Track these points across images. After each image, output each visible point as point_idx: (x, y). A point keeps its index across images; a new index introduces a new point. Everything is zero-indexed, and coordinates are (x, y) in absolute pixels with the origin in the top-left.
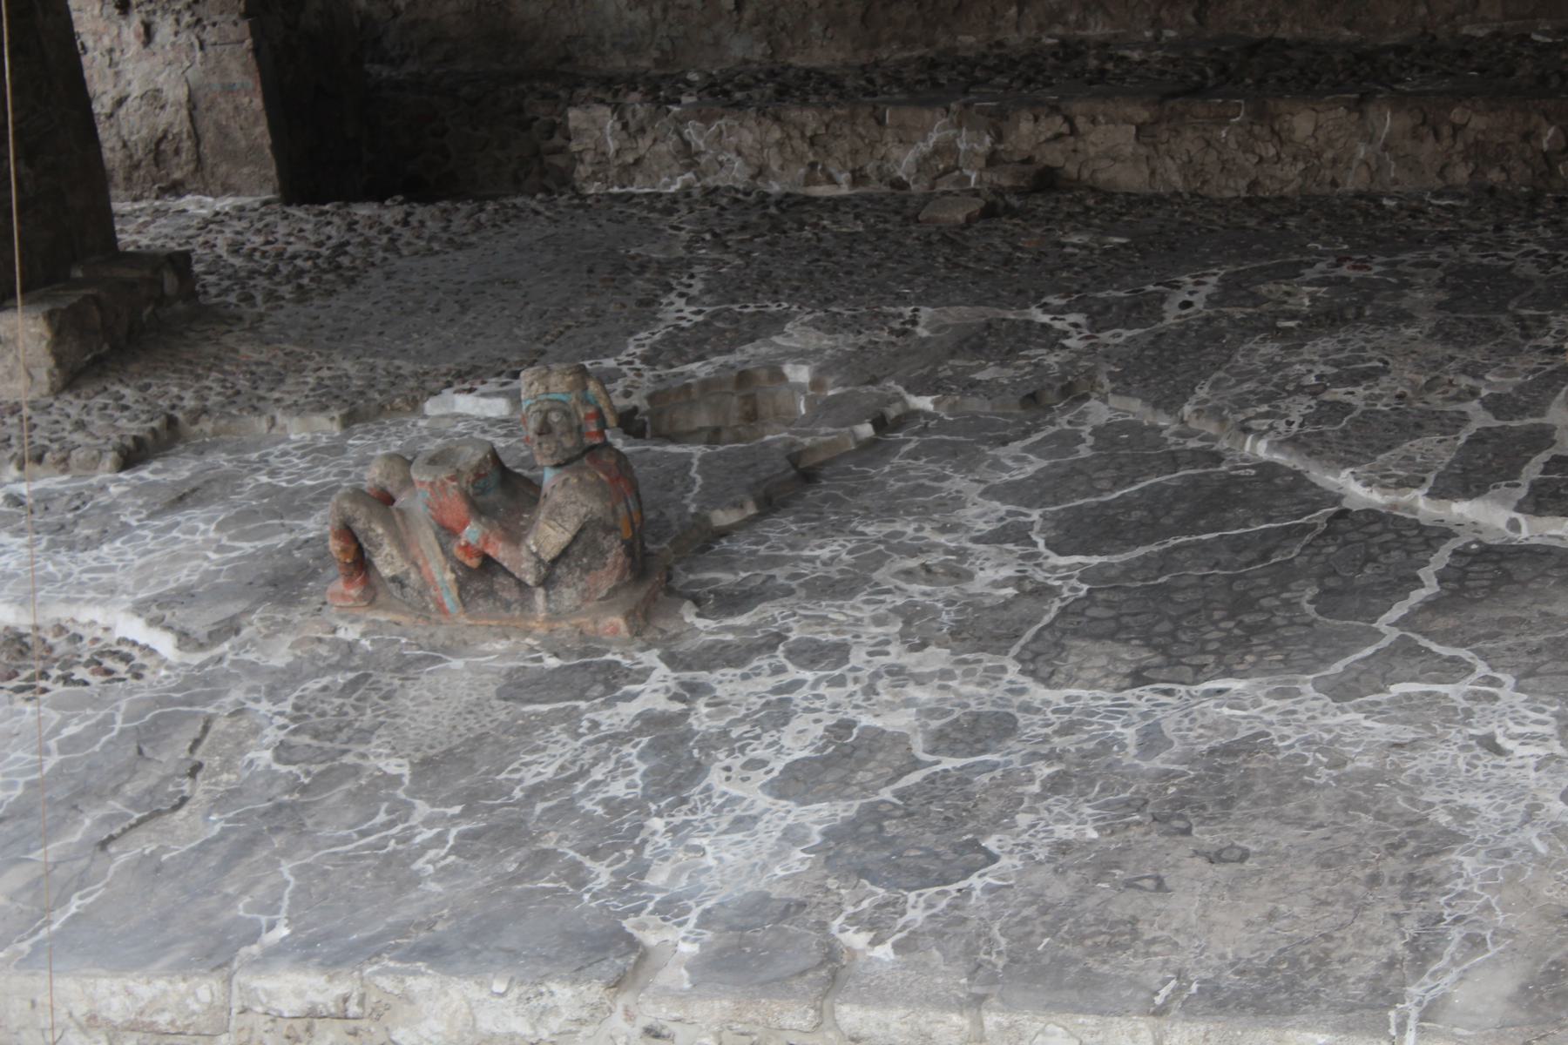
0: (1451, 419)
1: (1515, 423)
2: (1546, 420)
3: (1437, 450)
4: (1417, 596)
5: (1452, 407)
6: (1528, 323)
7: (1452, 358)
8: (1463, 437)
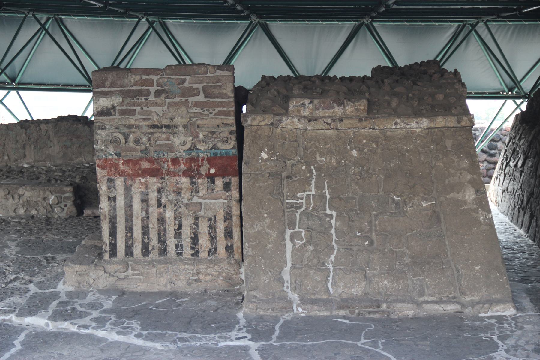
0: (24, 290)
1: (46, 291)
4: (13, 351)
6: (49, 258)
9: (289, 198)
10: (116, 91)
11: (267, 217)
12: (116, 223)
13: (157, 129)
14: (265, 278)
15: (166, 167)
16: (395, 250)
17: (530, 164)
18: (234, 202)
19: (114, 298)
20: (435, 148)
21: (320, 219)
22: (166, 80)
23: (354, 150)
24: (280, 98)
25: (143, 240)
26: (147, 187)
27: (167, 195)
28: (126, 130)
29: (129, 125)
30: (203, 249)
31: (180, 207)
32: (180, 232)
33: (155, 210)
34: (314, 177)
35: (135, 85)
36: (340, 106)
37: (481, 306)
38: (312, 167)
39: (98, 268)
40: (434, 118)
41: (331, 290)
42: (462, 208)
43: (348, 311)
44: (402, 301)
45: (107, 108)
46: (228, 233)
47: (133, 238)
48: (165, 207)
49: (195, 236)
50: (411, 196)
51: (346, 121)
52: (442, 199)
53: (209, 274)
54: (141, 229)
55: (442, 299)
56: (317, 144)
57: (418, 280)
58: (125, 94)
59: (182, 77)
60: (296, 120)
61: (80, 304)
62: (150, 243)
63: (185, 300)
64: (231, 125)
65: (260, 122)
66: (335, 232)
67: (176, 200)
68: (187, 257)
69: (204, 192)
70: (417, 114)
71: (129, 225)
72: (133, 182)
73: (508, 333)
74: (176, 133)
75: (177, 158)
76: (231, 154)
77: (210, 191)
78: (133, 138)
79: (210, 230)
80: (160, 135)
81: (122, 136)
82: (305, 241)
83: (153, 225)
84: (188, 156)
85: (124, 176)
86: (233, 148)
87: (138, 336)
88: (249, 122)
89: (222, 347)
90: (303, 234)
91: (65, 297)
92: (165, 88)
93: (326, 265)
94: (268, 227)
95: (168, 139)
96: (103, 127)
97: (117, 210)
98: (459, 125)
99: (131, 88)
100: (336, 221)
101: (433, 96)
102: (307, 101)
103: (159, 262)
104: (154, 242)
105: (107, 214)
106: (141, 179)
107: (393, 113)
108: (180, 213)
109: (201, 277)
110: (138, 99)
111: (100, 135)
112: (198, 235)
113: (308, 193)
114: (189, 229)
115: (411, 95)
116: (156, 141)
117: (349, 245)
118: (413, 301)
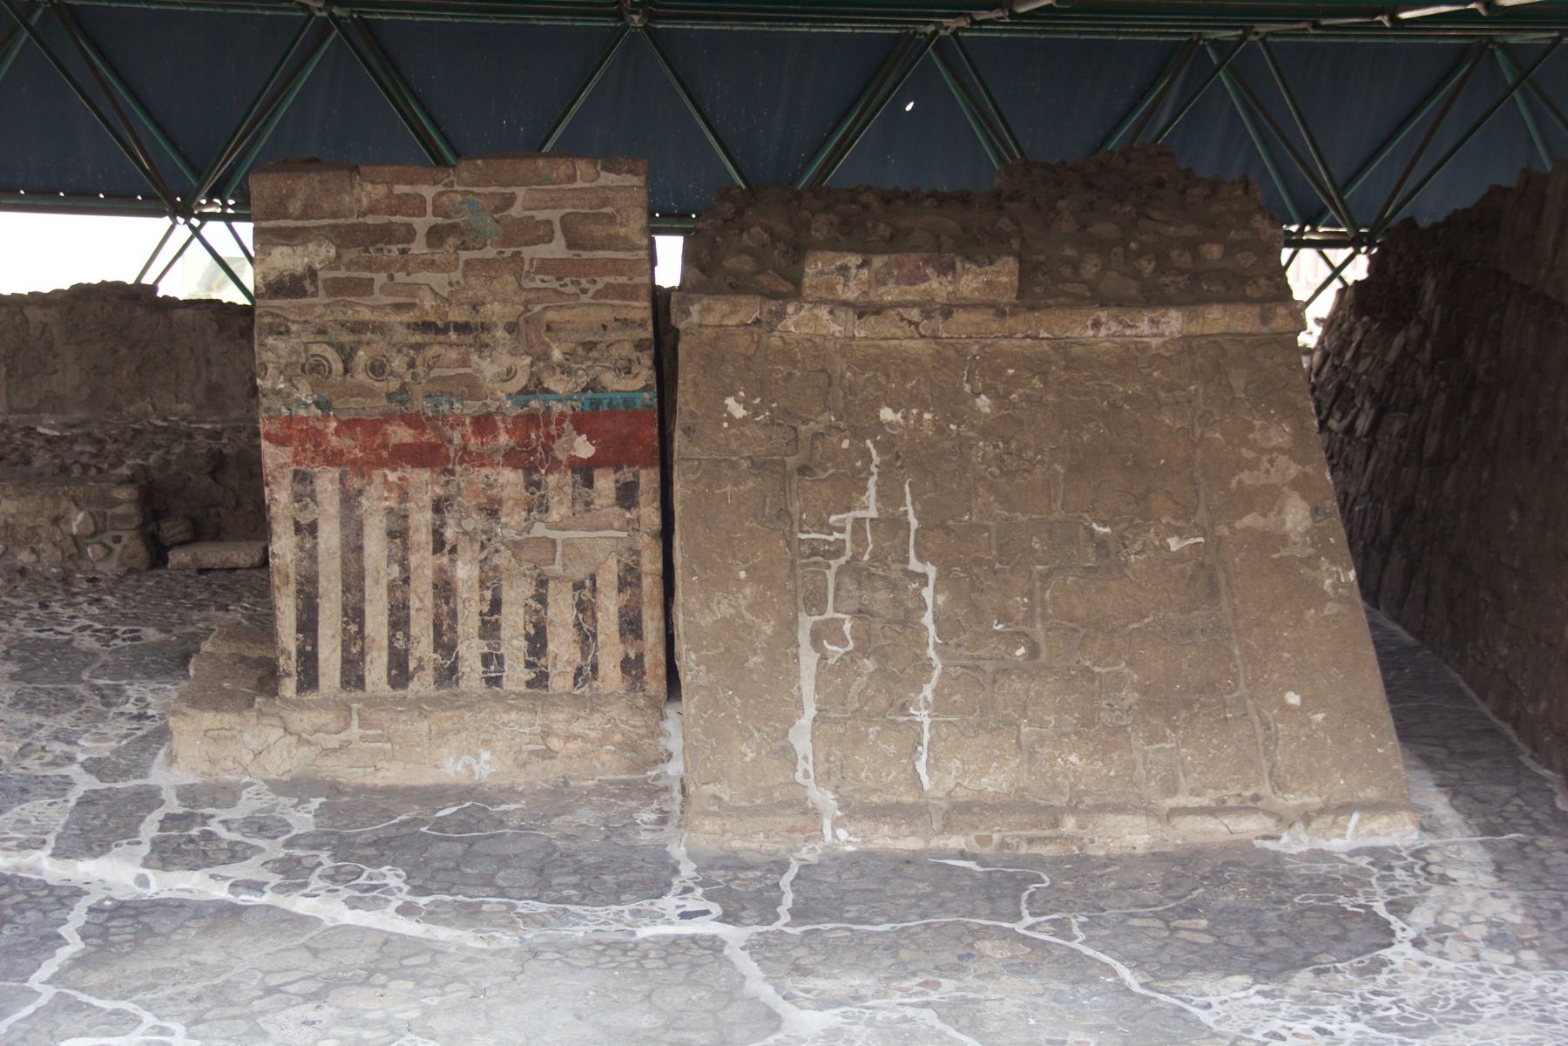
0: (56, 783)
1: (120, 785)
2: (150, 781)
3: (54, 814)
4: (63, 954)
5: (52, 772)
6: (106, 692)
7: (40, 726)
8: (73, 802)
9: (806, 528)
10: (318, 228)
11: (746, 580)
12: (317, 596)
13: (433, 336)
14: (743, 748)
15: (457, 439)
16: (1097, 669)
17: (1397, 426)
18: (647, 539)
19: (316, 803)
20: (1201, 391)
21: (893, 586)
22: (459, 198)
23: (983, 397)
24: (776, 252)
25: (391, 646)
26: (404, 496)
27: (460, 519)
28: (346, 338)
29: (356, 323)
30: (560, 665)
31: (497, 551)
32: (497, 620)
33: (425, 559)
34: (874, 469)
35: (371, 211)
36: (945, 275)
37: (1329, 819)
38: (869, 443)
39: (266, 721)
40: (1200, 308)
41: (925, 779)
42: (1276, 556)
43: (972, 838)
44: (1119, 809)
45: (292, 276)
46: (630, 623)
47: (363, 638)
48: (453, 550)
49: (537, 633)
50: (1137, 521)
51: (960, 317)
52: (1223, 530)
53: (575, 737)
54: (386, 613)
55: (1224, 802)
56: (882, 379)
57: (1158, 750)
58: (345, 237)
59: (503, 190)
60: (823, 312)
61: (224, 822)
62: (412, 651)
63: (512, 807)
64: (640, 325)
65: (723, 317)
66: (935, 621)
67: (485, 532)
68: (514, 688)
69: (564, 510)
70: (1155, 299)
71: (352, 600)
72: (365, 482)
73: (1411, 893)
74: (487, 346)
75: (488, 416)
76: (639, 406)
77: (578, 507)
78: (365, 358)
79: (581, 616)
80: (443, 351)
81: (336, 355)
82: (851, 645)
83: (421, 600)
84: (520, 411)
85: (339, 465)
86: (644, 389)
87: (406, 910)
88: (695, 318)
89: (646, 940)
90: (847, 627)
91: (176, 802)
92: (457, 220)
93: (912, 711)
94: (750, 607)
95: (464, 362)
96: (282, 329)
97: (320, 559)
98: (1265, 330)
99: (361, 220)
100: (936, 591)
101: (1192, 245)
102: (853, 260)
103: (436, 703)
104: (423, 648)
105: (292, 571)
106: (388, 472)
107: (1088, 294)
108: (496, 569)
109: (555, 743)
110: (381, 250)
111: (273, 349)
112: (545, 627)
113: (859, 514)
114: (521, 611)
115: (1133, 245)
116: (430, 368)
117: (972, 658)
118: (1149, 811)
